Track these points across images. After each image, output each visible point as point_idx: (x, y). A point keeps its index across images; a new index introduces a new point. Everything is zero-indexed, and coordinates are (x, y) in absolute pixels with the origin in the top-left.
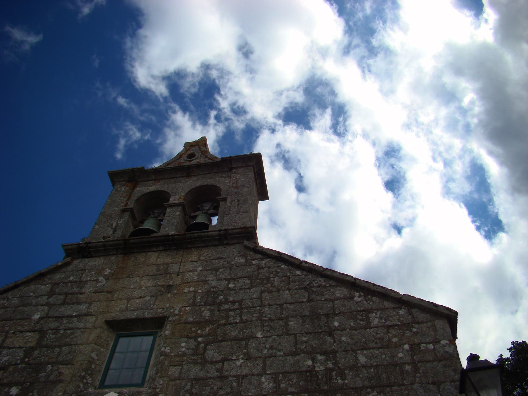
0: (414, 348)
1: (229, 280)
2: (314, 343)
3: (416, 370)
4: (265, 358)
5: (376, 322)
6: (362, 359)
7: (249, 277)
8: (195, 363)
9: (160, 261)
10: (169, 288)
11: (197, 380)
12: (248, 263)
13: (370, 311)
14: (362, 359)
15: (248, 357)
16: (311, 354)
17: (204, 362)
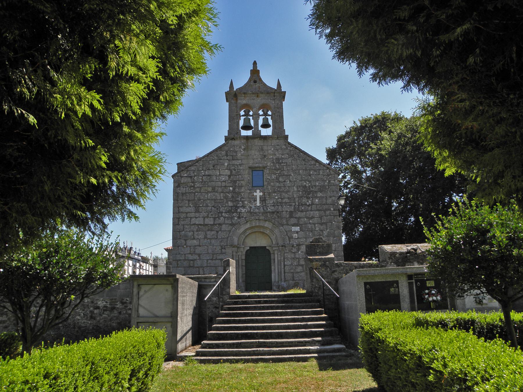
0: (329, 181)
1: (282, 154)
2: (306, 178)
3: (329, 188)
4: (294, 182)
5: (321, 173)
6: (317, 184)
7: (288, 154)
8: (277, 182)
9: (259, 144)
10: (265, 156)
11: (278, 187)
12: (287, 148)
13: (320, 170)
14: (317, 184)
15: (290, 181)
16: (305, 181)
17: (279, 182)
